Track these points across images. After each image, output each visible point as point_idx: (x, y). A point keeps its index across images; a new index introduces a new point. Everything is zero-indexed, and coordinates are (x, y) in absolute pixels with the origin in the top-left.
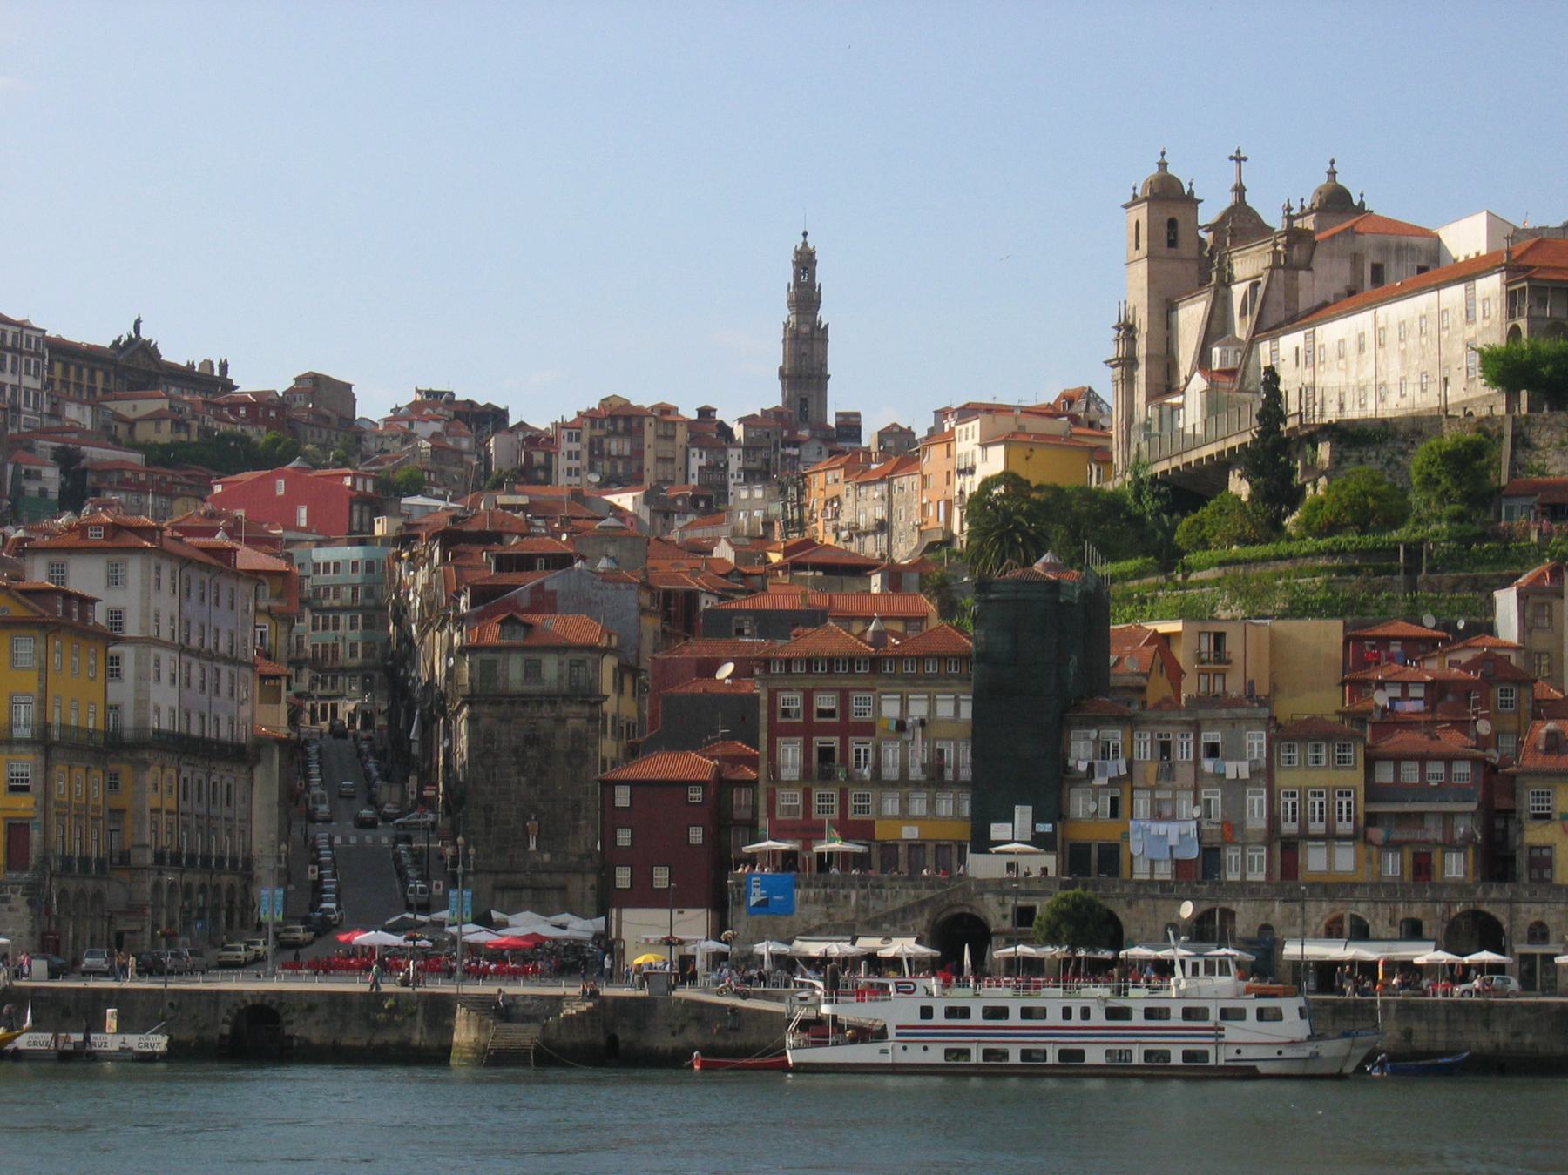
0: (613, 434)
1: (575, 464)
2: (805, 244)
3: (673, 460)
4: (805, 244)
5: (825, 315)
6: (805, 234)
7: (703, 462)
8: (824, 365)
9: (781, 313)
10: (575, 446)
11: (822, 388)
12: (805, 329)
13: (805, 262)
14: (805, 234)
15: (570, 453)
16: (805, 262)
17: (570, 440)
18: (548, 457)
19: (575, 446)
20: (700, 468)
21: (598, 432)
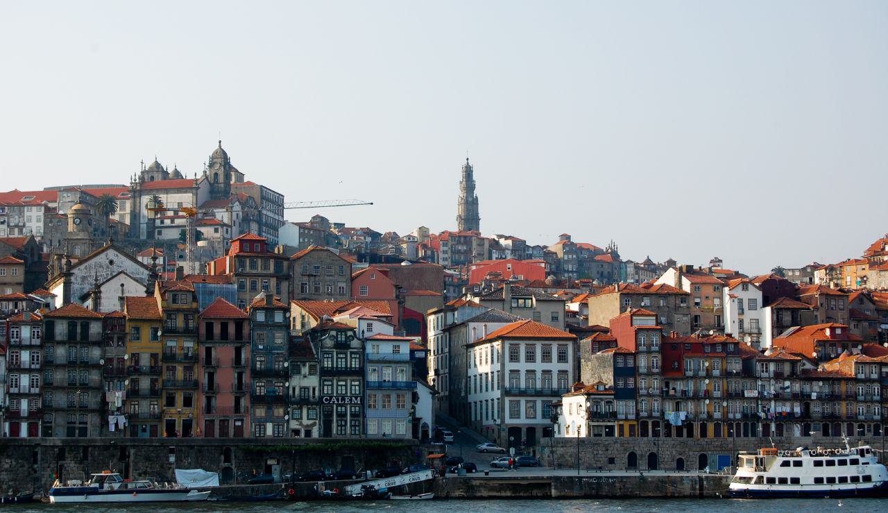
0: (459, 243)
1: (446, 256)
3: (483, 254)
5: (477, 192)
6: (468, 159)
8: (477, 214)
9: (456, 193)
10: (446, 248)
11: (478, 224)
12: (470, 199)
13: (468, 172)
15: (443, 251)
16: (468, 172)
17: (444, 246)
18: (433, 252)
19: (446, 248)
21: (454, 243)
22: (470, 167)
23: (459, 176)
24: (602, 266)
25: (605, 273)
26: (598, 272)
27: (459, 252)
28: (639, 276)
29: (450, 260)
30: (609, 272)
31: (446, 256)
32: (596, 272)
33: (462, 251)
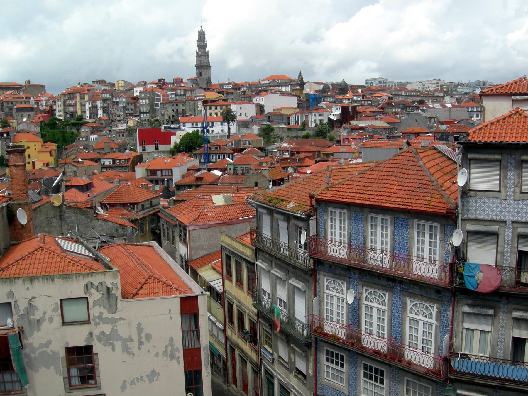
1: (60, 108)
2: (201, 29)
4: (201, 29)
6: (201, 27)
7: (90, 106)
10: (60, 103)
13: (202, 36)
14: (201, 27)
16: (202, 36)
20: (90, 108)
22: (203, 32)
23: (197, 38)
24: (177, 105)
25: (180, 111)
26: (173, 111)
27: (70, 105)
28: (206, 112)
29: (63, 112)
30: (183, 110)
31: (60, 108)
32: (171, 110)
33: (72, 104)
